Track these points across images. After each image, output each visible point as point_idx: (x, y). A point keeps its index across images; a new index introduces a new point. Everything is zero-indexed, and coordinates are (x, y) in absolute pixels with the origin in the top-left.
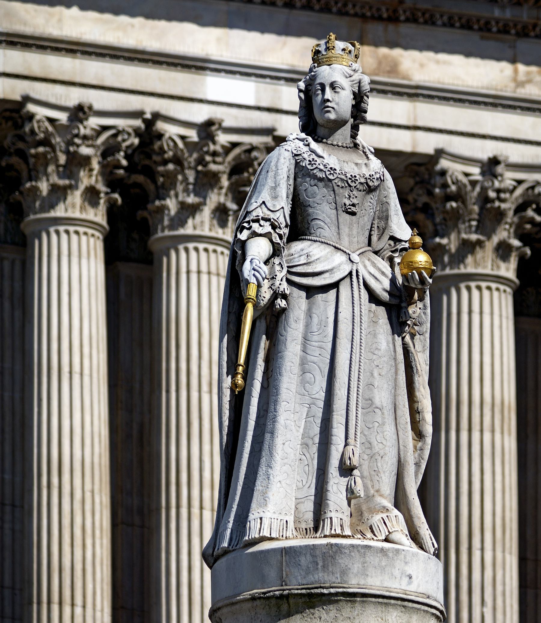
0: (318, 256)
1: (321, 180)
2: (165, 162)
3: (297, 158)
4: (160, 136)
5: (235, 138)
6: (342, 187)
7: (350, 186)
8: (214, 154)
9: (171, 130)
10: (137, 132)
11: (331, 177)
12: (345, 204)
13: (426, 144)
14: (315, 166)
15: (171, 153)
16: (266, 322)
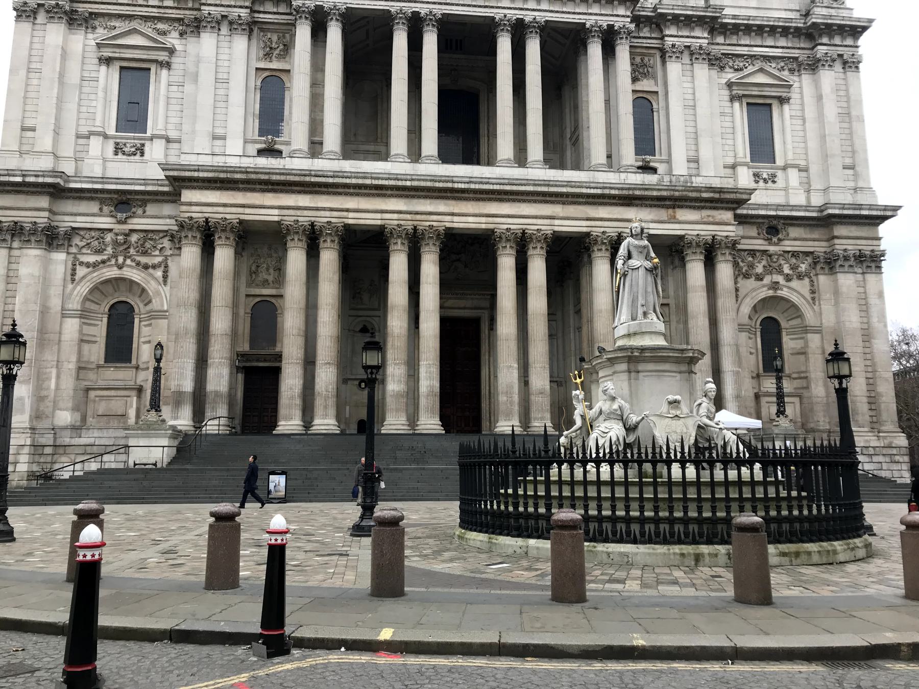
0: (634, 262)
13: (683, 233)
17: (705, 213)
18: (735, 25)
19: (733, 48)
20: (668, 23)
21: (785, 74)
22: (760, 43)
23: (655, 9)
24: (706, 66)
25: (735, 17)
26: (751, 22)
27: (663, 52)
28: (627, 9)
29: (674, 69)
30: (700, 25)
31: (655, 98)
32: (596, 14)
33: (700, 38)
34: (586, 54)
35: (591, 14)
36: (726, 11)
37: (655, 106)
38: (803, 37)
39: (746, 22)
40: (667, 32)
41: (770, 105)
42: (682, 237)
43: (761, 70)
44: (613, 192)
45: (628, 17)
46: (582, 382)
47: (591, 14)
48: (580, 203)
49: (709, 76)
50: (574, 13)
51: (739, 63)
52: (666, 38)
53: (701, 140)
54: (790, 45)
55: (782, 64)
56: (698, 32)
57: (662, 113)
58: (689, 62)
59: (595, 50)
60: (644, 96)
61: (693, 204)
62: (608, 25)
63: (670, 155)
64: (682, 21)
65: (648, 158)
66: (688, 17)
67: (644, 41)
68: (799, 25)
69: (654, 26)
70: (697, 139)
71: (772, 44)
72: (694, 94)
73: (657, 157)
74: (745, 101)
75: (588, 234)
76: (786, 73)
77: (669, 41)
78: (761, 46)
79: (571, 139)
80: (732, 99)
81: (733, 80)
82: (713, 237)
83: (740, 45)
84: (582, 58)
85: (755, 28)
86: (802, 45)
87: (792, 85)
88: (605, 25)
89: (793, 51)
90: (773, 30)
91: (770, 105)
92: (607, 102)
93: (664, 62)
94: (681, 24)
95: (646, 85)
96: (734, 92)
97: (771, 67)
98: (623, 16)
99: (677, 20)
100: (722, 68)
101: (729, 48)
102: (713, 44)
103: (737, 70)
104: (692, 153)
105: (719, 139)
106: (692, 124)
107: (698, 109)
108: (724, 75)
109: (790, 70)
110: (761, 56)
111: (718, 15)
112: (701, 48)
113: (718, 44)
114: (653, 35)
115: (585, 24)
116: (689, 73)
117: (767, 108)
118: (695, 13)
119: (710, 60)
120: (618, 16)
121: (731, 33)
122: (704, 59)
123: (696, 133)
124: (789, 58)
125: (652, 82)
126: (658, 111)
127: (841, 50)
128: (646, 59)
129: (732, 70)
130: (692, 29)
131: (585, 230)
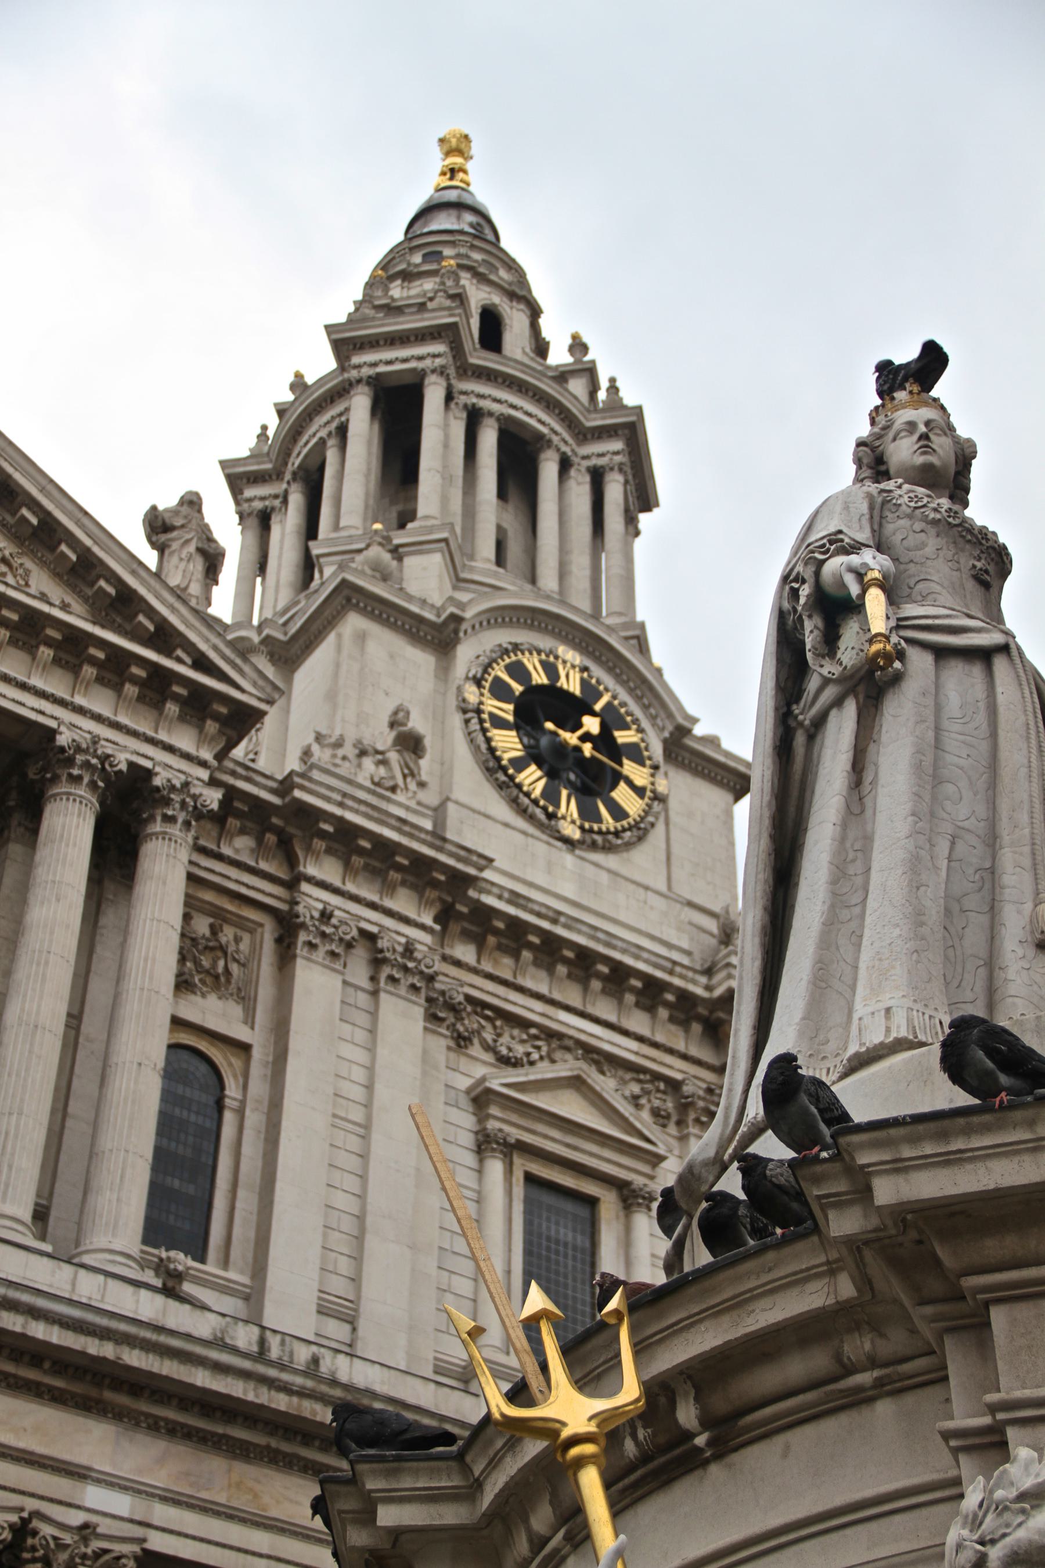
1: (935, 522)
3: (885, 495)
4: (35, 1533)
5: (105, 1545)
6: (969, 541)
7: (981, 544)
8: (84, 1556)
9: (47, 1530)
10: (12, 1526)
11: (950, 520)
12: (974, 566)
14: (920, 504)
15: (42, 1552)
16: (857, 703)
19: (501, 990)
20: (319, 844)
21: (643, 1120)
22: (576, 1002)
23: (286, 786)
24: (418, 1012)
25: (515, 898)
26: (560, 931)
27: (288, 926)
28: (202, 738)
31: (237, 1063)
32: (98, 718)
33: (407, 920)
34: (35, 831)
36: (487, 874)
37: (232, 1090)
38: (697, 1028)
39: (545, 925)
40: (311, 870)
41: (592, 1202)
43: (577, 1083)
44: (39, 1330)
45: (203, 764)
46: (611, 1432)
49: (425, 1051)
50: (23, 686)
51: (512, 1043)
52: (305, 887)
53: (372, 1242)
54: (659, 1038)
55: (636, 1089)
56: (403, 902)
57: (254, 1119)
58: (365, 984)
59: (70, 828)
60: (203, 1045)
62: (131, 765)
63: (259, 1268)
64: (361, 852)
65: (181, 1260)
66: (382, 846)
67: (233, 872)
68: (691, 988)
69: (271, 838)
70: (360, 1239)
71: (612, 1018)
72: (369, 1087)
73: (210, 1267)
74: (521, 1165)
76: (646, 1115)
77: (313, 900)
80: (485, 1144)
81: (495, 1085)
85: (569, 954)
86: (694, 1051)
87: (661, 1158)
88: (122, 761)
89: (668, 1059)
90: (618, 978)
91: (592, 1202)
92: (75, 1020)
94: (357, 861)
95: (213, 1012)
96: (492, 1125)
97: (606, 1084)
98: (187, 757)
99: (345, 840)
100: (461, 1041)
101: (490, 986)
102: (445, 958)
103: (507, 1061)
104: (339, 1286)
105: (430, 1264)
106: (351, 1183)
107: (376, 1136)
108: (464, 1063)
109: (656, 1113)
111: (472, 871)
112: (409, 950)
113: (458, 963)
114: (263, 865)
115: (52, 733)
116: (363, 1019)
117: (583, 1212)
118: (405, 841)
119: (429, 1000)
120: (170, 749)
121: (500, 948)
122: (414, 988)
123: (361, 1218)
124: (657, 1077)
125: (236, 1010)
126: (241, 1112)
128: (227, 934)
130: (389, 889)
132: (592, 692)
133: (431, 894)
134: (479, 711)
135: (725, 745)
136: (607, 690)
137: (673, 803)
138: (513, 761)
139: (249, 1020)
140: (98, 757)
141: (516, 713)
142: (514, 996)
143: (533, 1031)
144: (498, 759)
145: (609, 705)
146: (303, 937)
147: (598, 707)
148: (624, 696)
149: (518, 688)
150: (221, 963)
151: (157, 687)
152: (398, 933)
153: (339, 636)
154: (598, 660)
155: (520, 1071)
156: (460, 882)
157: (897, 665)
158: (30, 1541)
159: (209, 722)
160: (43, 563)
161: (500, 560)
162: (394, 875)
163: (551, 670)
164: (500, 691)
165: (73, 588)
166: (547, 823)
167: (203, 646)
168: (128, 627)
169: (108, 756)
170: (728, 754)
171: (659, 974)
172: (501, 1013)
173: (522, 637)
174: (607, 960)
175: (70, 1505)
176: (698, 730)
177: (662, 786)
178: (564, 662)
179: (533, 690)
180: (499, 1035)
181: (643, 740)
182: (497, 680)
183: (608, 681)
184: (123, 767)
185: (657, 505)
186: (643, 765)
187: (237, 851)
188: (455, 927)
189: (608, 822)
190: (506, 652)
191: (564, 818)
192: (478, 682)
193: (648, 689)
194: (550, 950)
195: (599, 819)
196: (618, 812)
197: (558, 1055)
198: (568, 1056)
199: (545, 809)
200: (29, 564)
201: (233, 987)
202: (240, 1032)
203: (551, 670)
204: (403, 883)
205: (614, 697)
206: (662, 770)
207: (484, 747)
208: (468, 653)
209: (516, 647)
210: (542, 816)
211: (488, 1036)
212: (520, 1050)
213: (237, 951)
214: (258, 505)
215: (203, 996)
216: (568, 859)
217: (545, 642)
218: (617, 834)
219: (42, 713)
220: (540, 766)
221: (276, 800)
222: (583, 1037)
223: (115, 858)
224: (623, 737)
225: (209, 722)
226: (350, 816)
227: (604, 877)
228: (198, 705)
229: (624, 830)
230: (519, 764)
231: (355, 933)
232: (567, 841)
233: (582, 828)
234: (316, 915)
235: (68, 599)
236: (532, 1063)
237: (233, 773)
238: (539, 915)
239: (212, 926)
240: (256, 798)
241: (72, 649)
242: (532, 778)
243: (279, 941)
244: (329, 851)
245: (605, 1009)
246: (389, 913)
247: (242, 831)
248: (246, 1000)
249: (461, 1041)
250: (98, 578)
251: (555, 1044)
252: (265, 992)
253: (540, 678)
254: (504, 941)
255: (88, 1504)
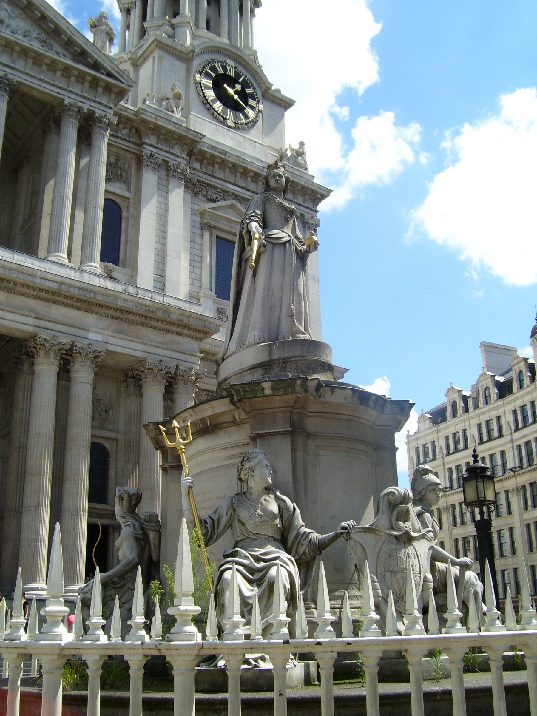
2: (77, 353)
17: (170, 337)
18: (212, 156)
19: (208, 177)
23: (136, 114)
25: (213, 147)
26: (227, 158)
27: (139, 159)
29: (150, 179)
30: (180, 145)
35: (71, 92)
36: (204, 140)
39: (223, 156)
40: (147, 141)
42: (141, 361)
43: (232, 207)
45: (111, 108)
47: (71, 92)
48: (28, 296)
50: (53, 85)
52: (145, 146)
56: (176, 150)
59: (70, 132)
61: (159, 324)
66: (168, 131)
67: (122, 142)
75: (34, 336)
77: (147, 150)
78: (234, 185)
79: (22, 227)
82: (177, 366)
83: (215, 177)
84: (54, 137)
88: (86, 107)
93: (139, 169)
95: (118, 189)
110: (233, 194)
111: (199, 140)
112: (178, 166)
113: (194, 169)
114: (131, 139)
120: (100, 103)
125: (124, 187)
127: (303, 210)
129: (204, 199)
130: (171, 147)
131: (31, 329)
132: (238, 74)
133: (187, 147)
134: (200, 84)
135: (283, 93)
136: (243, 75)
137: (265, 113)
138: (212, 100)
139: (129, 190)
140: (77, 108)
141: (213, 84)
142: (213, 179)
143: (219, 190)
144: (207, 100)
145: (244, 79)
146: (145, 162)
147: (240, 81)
148: (249, 76)
149: (213, 75)
150: (119, 172)
151: (95, 83)
152: (175, 160)
153: (154, 58)
154: (240, 64)
155: (215, 204)
156: (194, 142)
157: (264, 249)
158: (75, 348)
159: (112, 94)
160: (56, 41)
161: (208, 29)
162: (173, 141)
163: (224, 68)
164: (208, 75)
165: (66, 49)
166: (223, 121)
167: (109, 69)
168: (85, 62)
169: (81, 107)
170: (283, 96)
171: (259, 171)
172: (208, 185)
173: (216, 57)
174: (242, 167)
175: (85, 338)
176: (273, 88)
177: (261, 107)
178: (229, 65)
179: (218, 75)
180: (208, 192)
181: (255, 92)
182: (207, 72)
183: (244, 71)
184: (86, 111)
185: (261, 5)
186: (255, 100)
187: (123, 135)
188: (193, 158)
189: (244, 121)
190: (210, 63)
191: (229, 119)
192: (201, 74)
193: (257, 75)
194: (224, 164)
195: (241, 119)
196: (247, 117)
197: (227, 198)
198: (230, 198)
199: (222, 117)
200: (52, 42)
201: (123, 179)
202: (126, 194)
203: (224, 68)
204: (176, 143)
205: (246, 77)
206: (261, 102)
207: (202, 95)
208: (197, 63)
209: (213, 61)
210: (222, 119)
211: (205, 193)
212: (214, 197)
213: (124, 167)
214: (127, 6)
215: (114, 182)
216: (231, 133)
217: (222, 58)
218: (246, 124)
219: (59, 93)
220: (221, 102)
221: (135, 118)
222: (235, 192)
223: (85, 140)
224: (249, 91)
225: (112, 94)
226: (158, 122)
227: (242, 139)
228: (108, 89)
229: (248, 123)
230: (214, 101)
231: (161, 161)
232: (230, 127)
233: (235, 123)
234: (149, 155)
235: (65, 53)
236: (218, 201)
237: (121, 109)
238: (220, 153)
239: (116, 159)
240: (128, 117)
241: (67, 71)
242: (218, 106)
243: (138, 163)
244: (152, 134)
245: (242, 183)
246: (172, 154)
247: (124, 128)
248: (127, 183)
249: (196, 194)
250: (75, 45)
251: (226, 194)
252: (133, 181)
253: (221, 71)
254: (209, 161)
255: (90, 338)
